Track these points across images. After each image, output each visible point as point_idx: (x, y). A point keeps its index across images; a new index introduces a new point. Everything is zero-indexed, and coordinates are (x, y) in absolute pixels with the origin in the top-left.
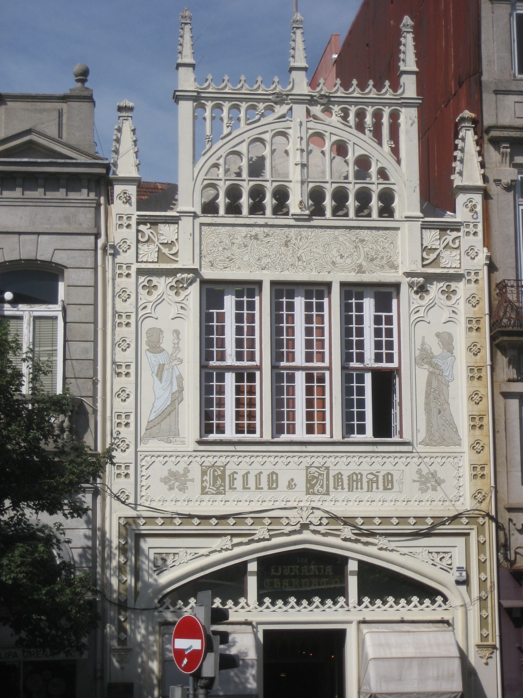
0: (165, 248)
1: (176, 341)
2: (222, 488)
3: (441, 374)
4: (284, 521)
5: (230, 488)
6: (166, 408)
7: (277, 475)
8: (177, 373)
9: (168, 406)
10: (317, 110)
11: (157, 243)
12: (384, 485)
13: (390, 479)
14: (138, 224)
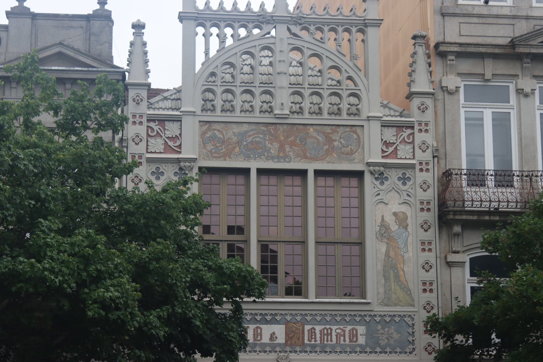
0: (170, 141)
3: (397, 246)
10: (296, 29)
11: (164, 137)
12: (350, 338)
13: (355, 333)
14: (149, 121)
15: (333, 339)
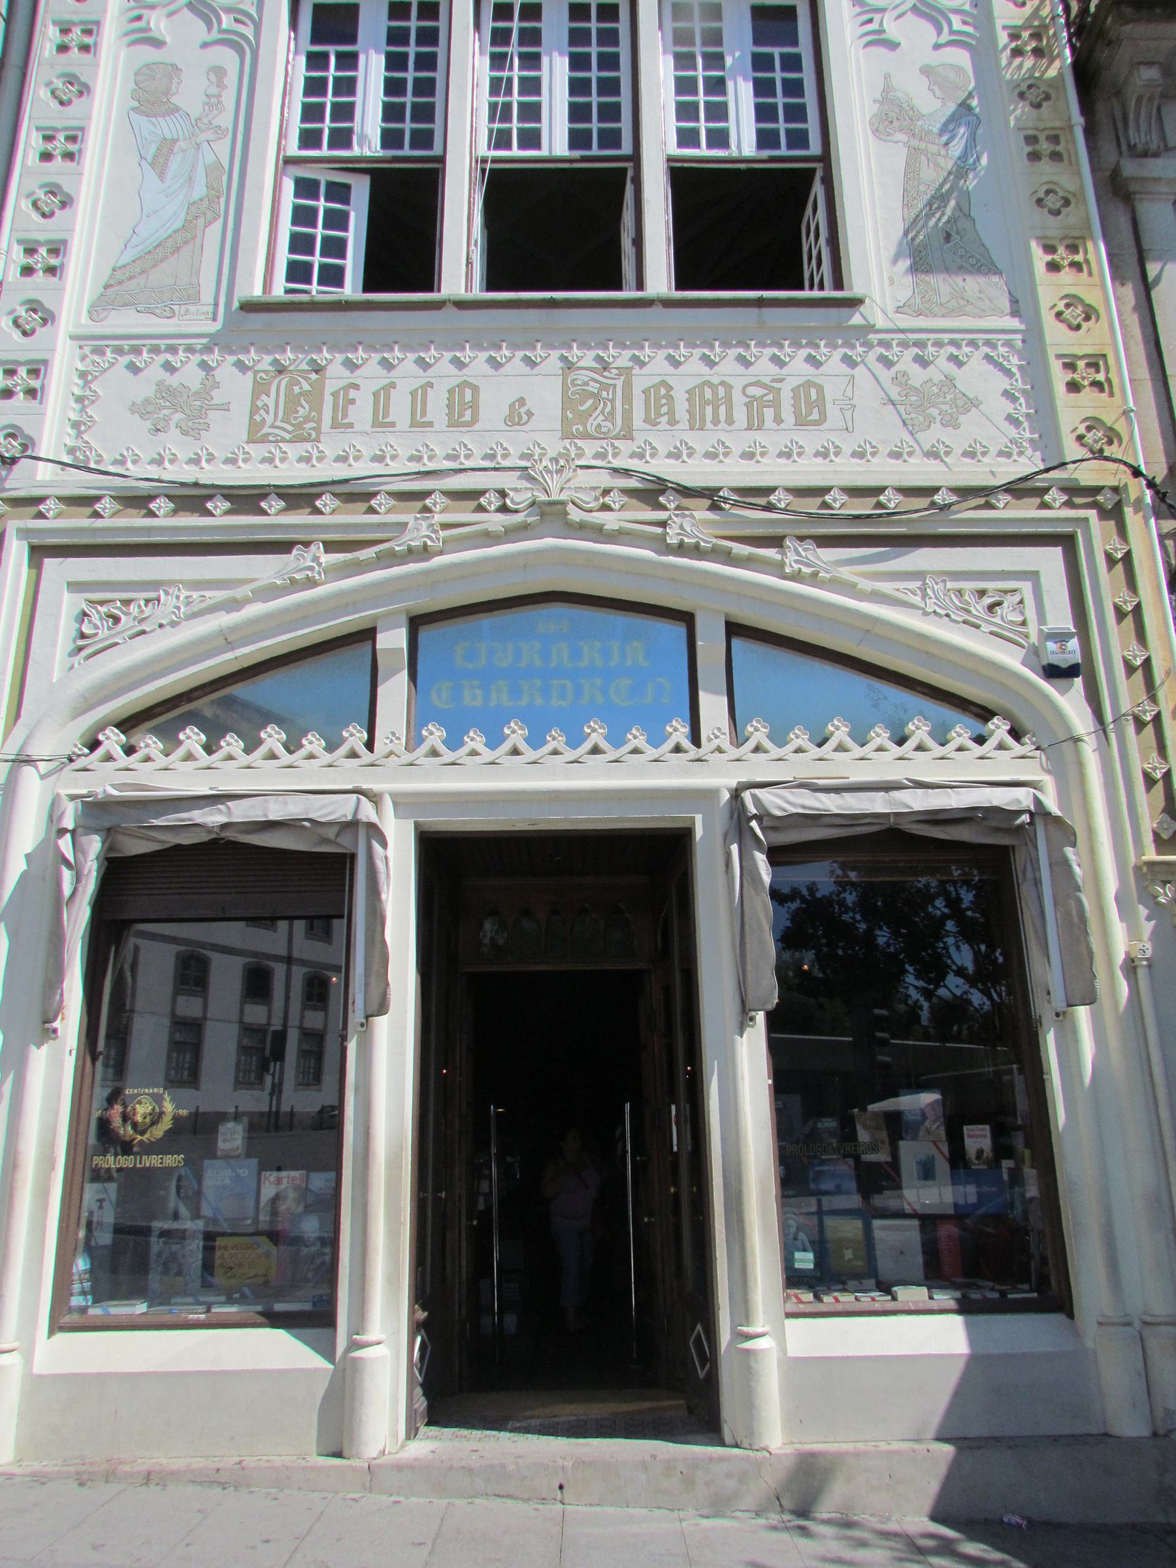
1: (214, 90)
2: (308, 426)
4: (491, 501)
5: (335, 425)
6: (170, 236)
7: (475, 389)
8: (210, 158)
9: (175, 232)
13: (814, 396)
15: (735, 417)
